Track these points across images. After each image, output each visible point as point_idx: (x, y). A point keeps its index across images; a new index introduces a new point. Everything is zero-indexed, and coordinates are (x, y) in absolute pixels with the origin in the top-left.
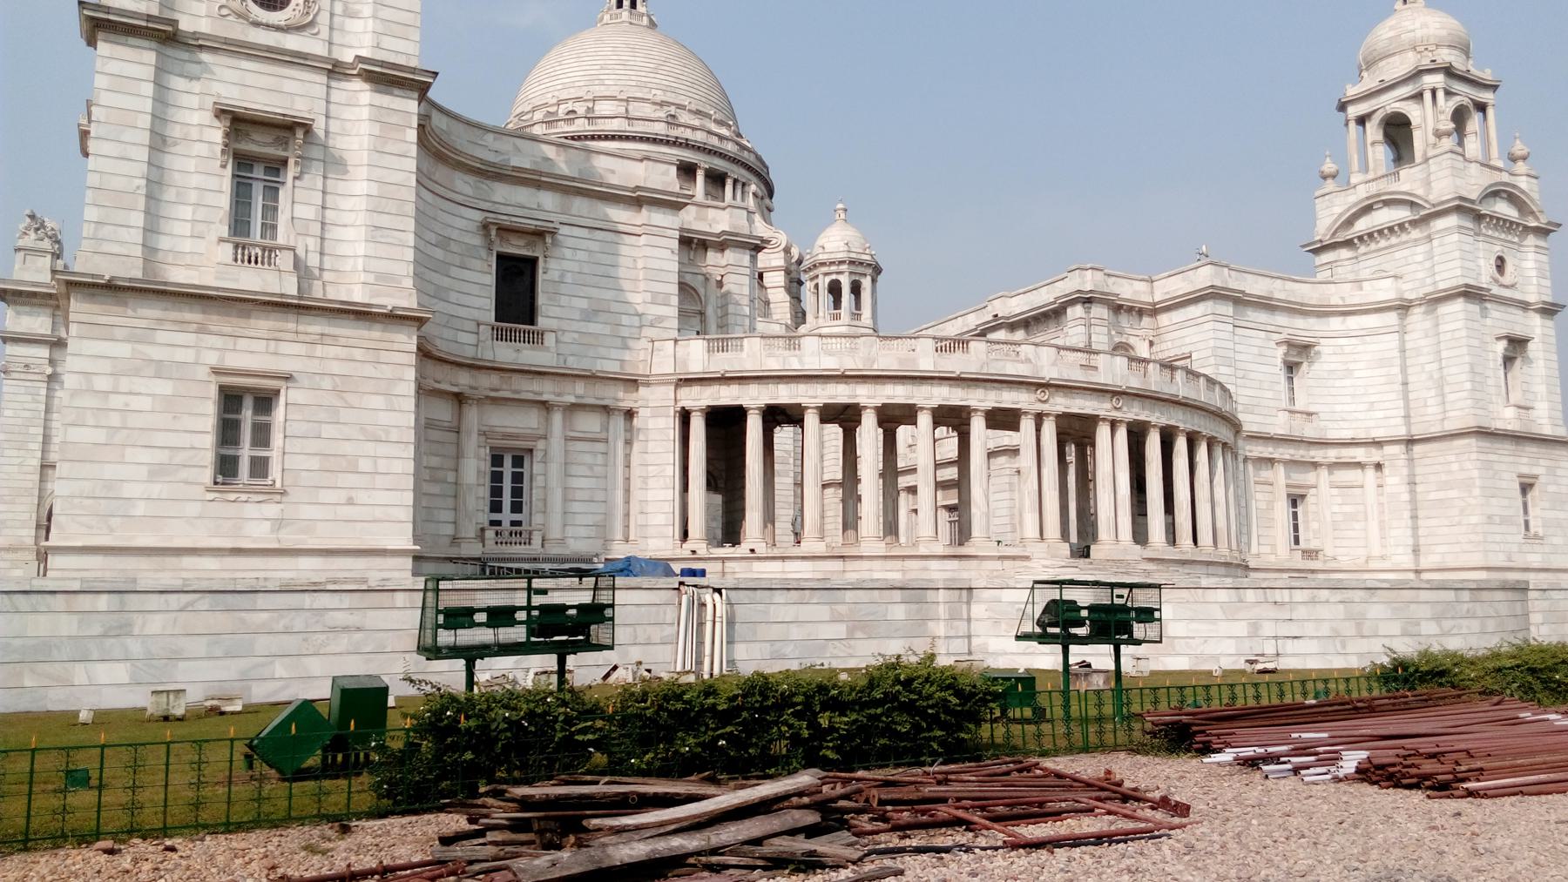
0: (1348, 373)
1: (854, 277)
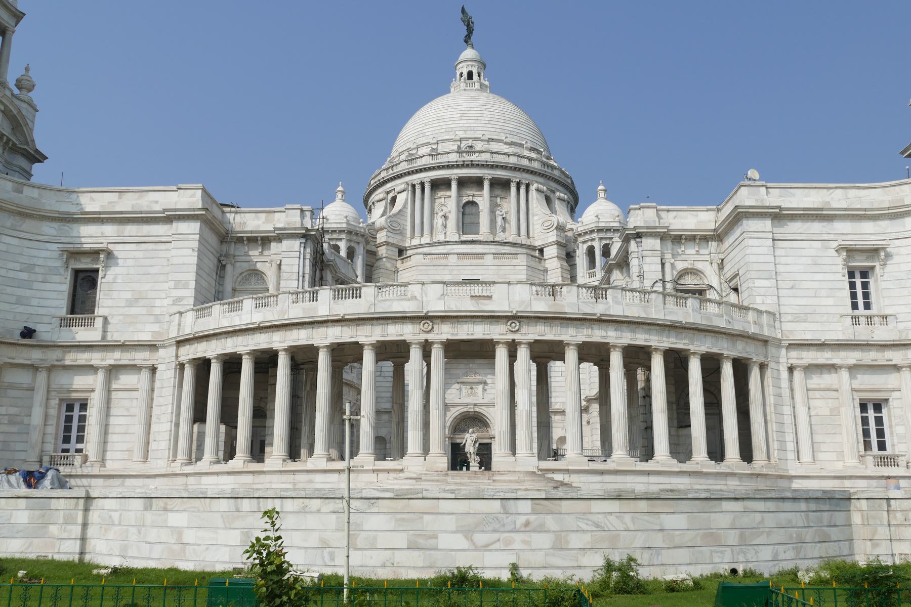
1: (604, 242)
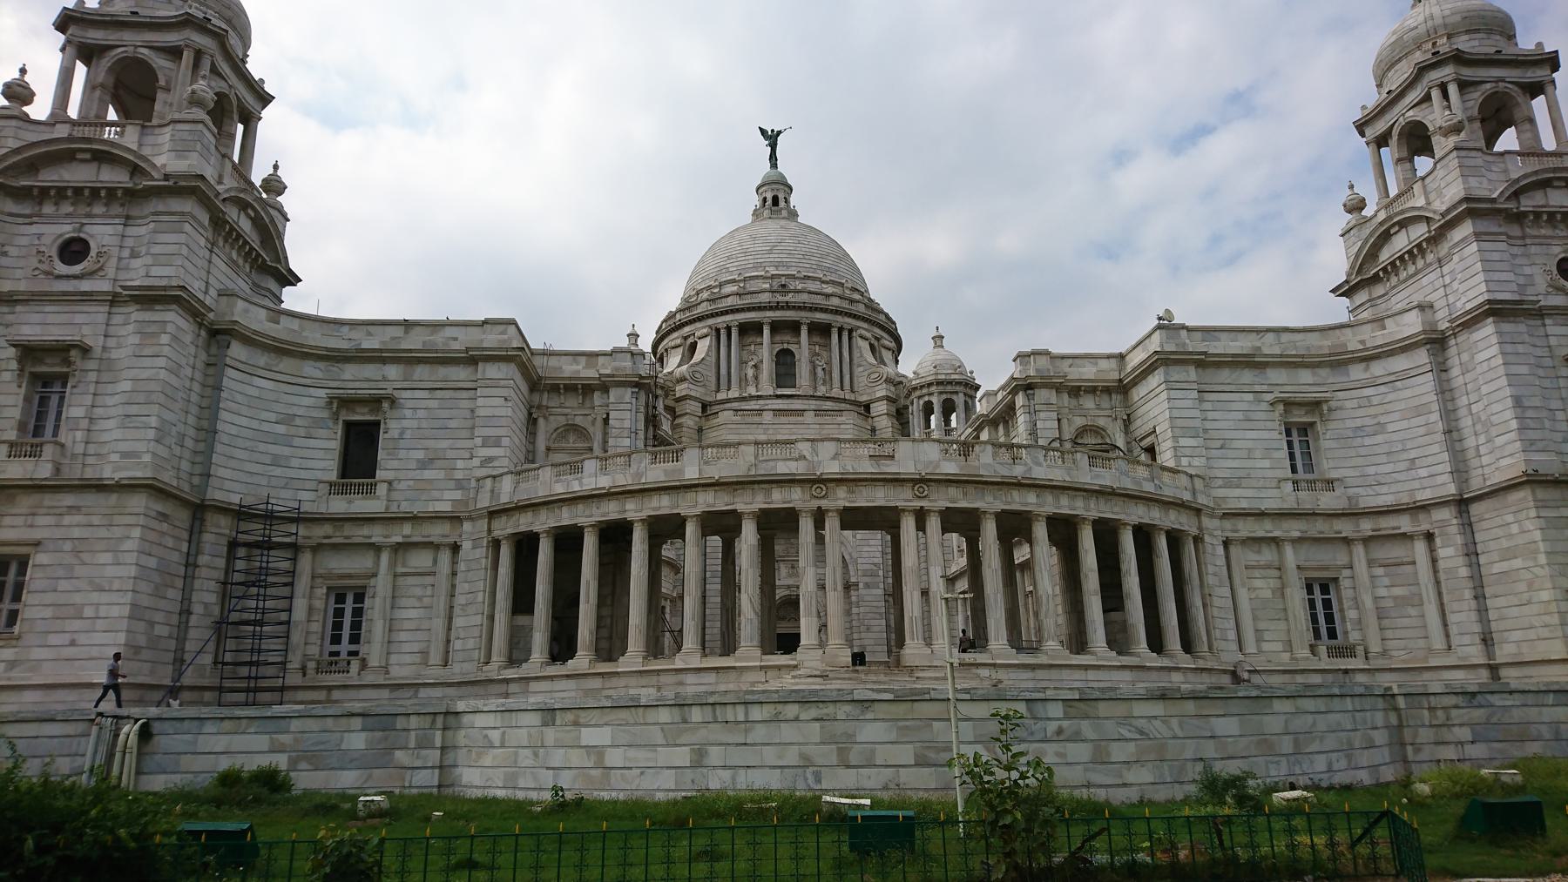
0: (1381, 428)
1: (944, 396)
